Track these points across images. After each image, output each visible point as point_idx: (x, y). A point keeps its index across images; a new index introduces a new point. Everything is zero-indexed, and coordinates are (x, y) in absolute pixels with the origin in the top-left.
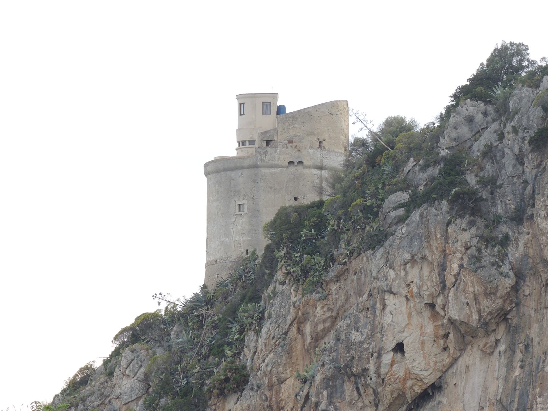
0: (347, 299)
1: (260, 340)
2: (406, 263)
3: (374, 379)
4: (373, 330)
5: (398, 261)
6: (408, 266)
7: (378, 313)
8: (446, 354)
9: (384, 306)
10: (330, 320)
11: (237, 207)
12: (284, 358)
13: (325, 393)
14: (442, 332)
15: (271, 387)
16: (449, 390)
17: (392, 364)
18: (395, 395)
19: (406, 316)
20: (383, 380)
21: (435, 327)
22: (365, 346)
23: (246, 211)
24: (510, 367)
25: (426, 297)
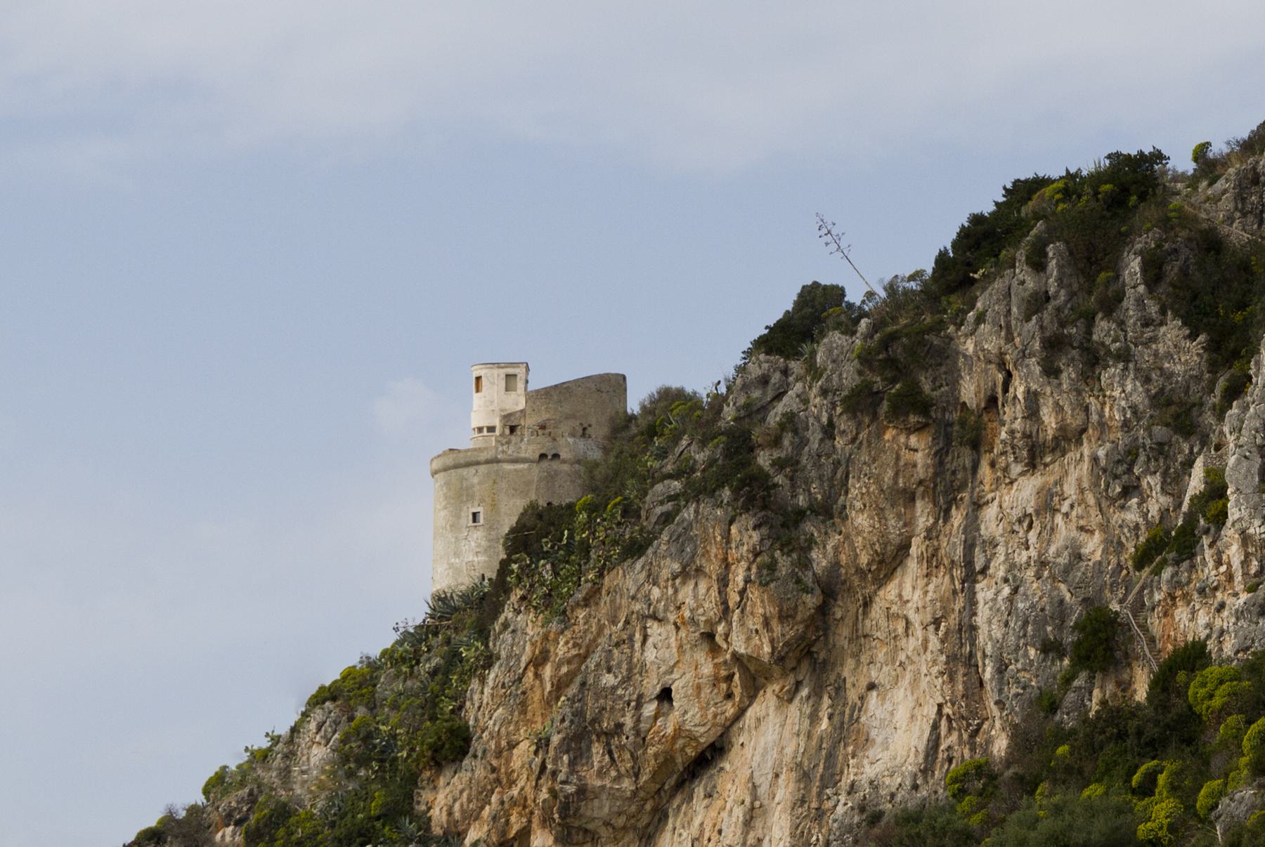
0: (601, 629)
1: (486, 690)
2: (674, 578)
3: (631, 738)
4: (630, 670)
5: (665, 574)
6: (678, 581)
7: (637, 645)
8: (730, 704)
9: (645, 638)
10: (576, 660)
11: (471, 517)
12: (516, 713)
13: (565, 758)
14: (723, 673)
15: (499, 754)
16: (735, 753)
17: (656, 717)
18: (661, 759)
19: (675, 650)
20: (644, 739)
21: (716, 666)
22: (620, 692)
23: (482, 521)
24: (814, 718)
25: (702, 625)
